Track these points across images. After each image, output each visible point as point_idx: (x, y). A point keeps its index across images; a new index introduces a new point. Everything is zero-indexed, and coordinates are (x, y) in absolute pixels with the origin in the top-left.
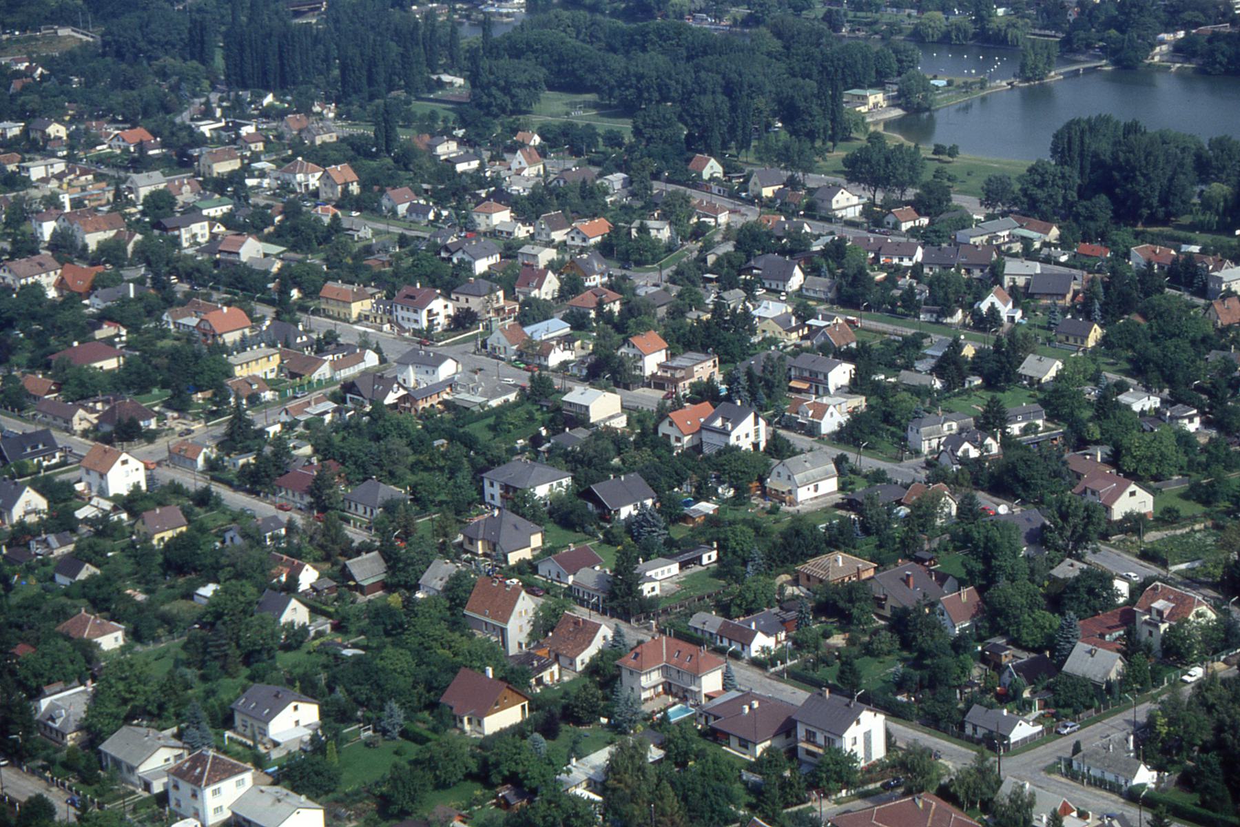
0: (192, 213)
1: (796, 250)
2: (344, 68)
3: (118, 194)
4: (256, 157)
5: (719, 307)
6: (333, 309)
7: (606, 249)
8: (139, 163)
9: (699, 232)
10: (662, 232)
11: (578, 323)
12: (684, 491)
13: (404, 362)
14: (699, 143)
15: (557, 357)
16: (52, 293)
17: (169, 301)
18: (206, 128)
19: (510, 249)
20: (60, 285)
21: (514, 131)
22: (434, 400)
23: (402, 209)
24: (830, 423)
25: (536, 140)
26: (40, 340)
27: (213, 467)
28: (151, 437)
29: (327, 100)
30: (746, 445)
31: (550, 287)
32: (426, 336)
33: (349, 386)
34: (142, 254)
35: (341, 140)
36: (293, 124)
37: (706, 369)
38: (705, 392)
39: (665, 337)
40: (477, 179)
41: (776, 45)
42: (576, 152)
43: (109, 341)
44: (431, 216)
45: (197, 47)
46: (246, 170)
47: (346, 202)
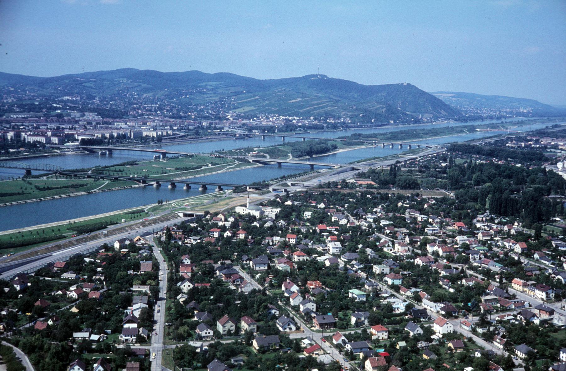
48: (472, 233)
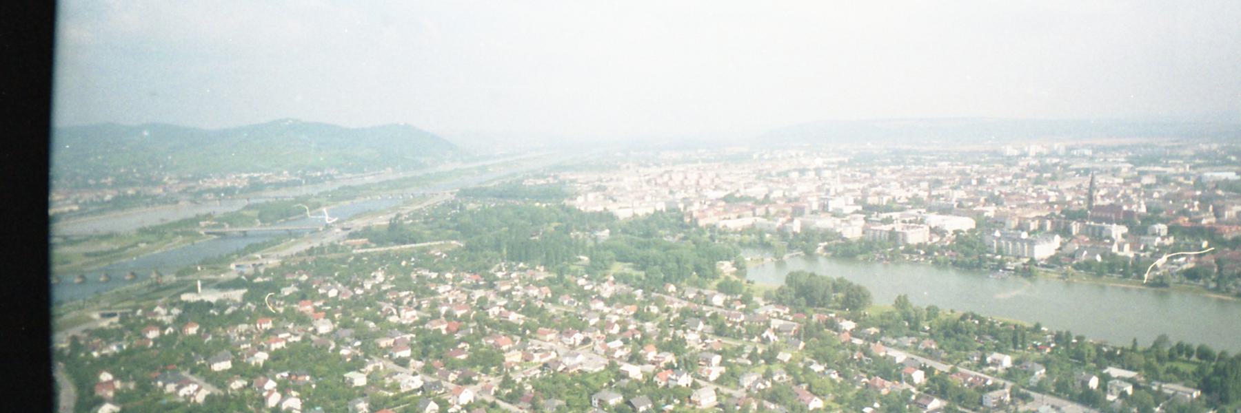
0: (493, 304)
1: (701, 316)
2: (547, 254)
3: (469, 297)
4: (516, 284)
5: (674, 337)
6: (541, 337)
7: (636, 316)
8: (476, 287)
9: (667, 310)
10: (655, 310)
11: (626, 342)
12: (663, 401)
13: (565, 356)
14: (667, 280)
15: (617, 355)
16: (444, 332)
17: (484, 335)
18: (499, 275)
19: (602, 317)
20: (447, 329)
21: (605, 275)
22: (575, 369)
23: (566, 302)
24: (713, 377)
25: (612, 278)
26: (439, 348)
27: (497, 394)
28: (476, 383)
29: (541, 265)
30: (684, 385)
31: (616, 330)
32: (572, 347)
33: (545, 365)
34: (476, 319)
35: (547, 278)
36: (528, 275)
37: (669, 358)
38: (670, 367)
39: (656, 347)
40: (591, 291)
41: (693, 246)
42: (625, 283)
43: (463, 349)
44: (576, 304)
45: (498, 247)
46: (513, 289)
47: (546, 300)
48: (491, 285)
